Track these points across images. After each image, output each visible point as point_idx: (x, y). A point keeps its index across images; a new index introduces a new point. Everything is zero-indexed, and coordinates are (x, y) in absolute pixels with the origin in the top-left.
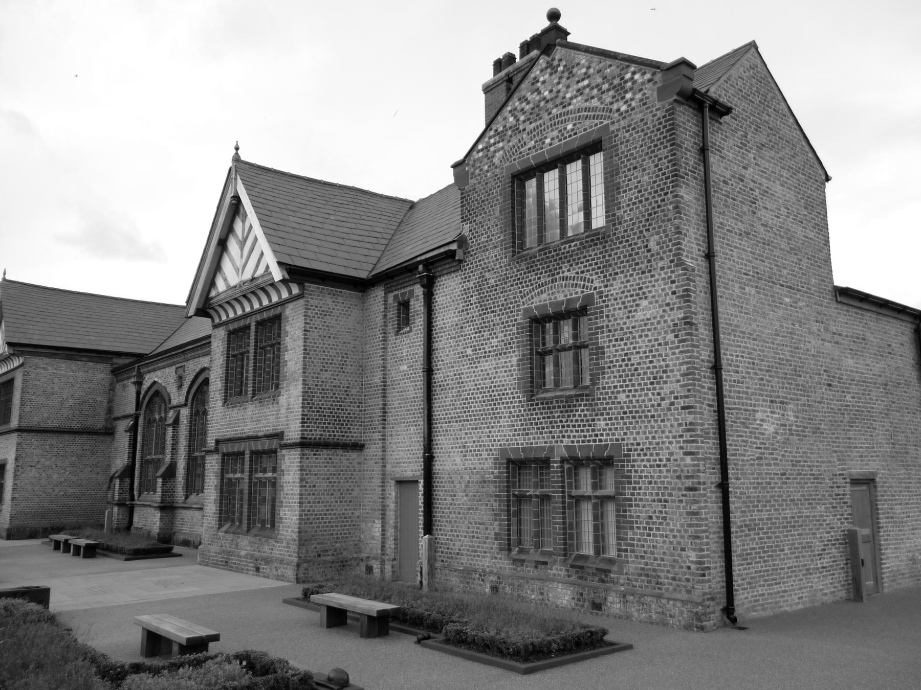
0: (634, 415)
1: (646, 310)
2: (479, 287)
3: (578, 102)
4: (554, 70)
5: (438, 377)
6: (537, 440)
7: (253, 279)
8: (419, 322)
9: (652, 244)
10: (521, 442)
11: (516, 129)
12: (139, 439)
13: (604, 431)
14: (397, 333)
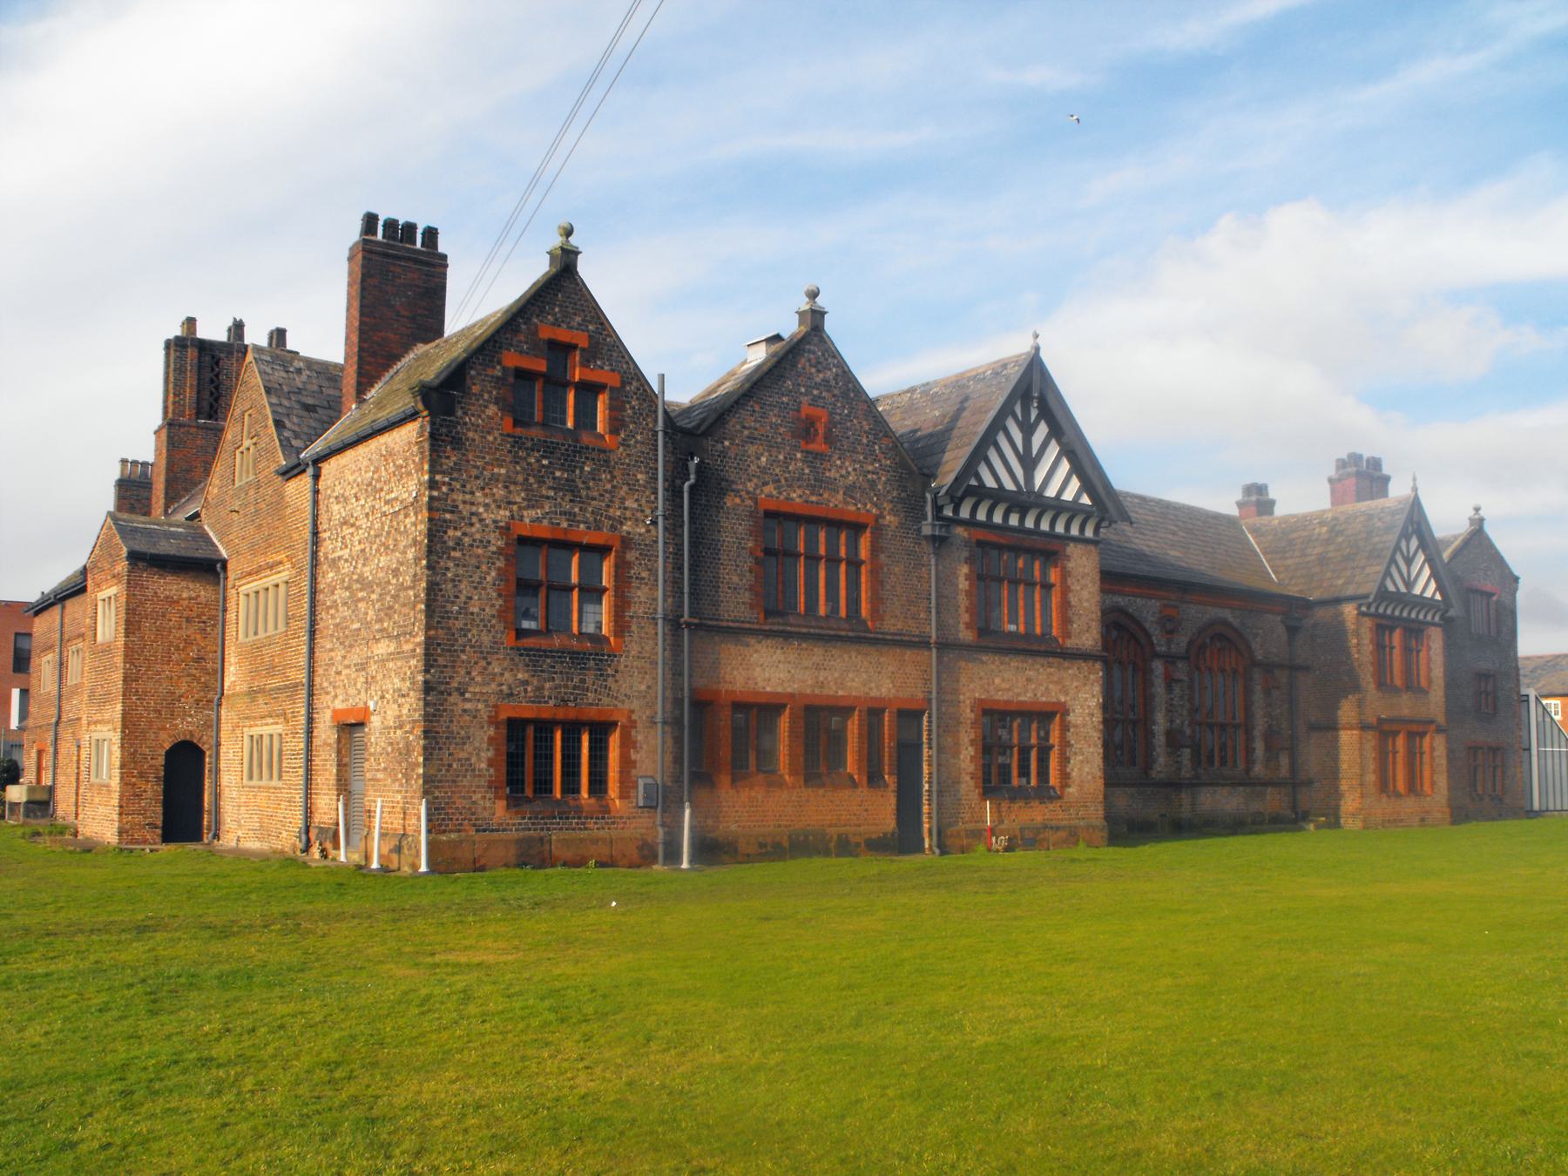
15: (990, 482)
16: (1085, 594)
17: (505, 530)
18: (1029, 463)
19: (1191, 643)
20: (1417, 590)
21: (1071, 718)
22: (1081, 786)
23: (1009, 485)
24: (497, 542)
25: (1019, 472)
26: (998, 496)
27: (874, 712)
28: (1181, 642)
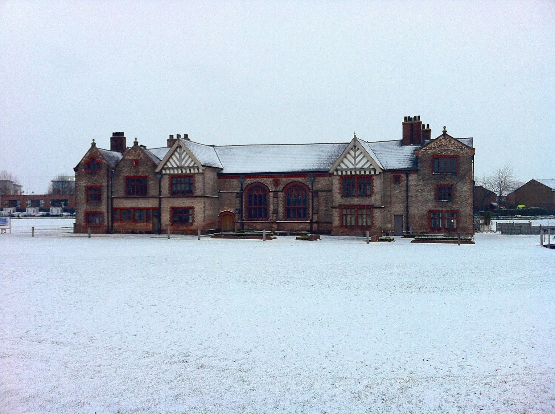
0: (461, 205)
1: (465, 189)
2: (424, 177)
3: (451, 148)
4: (446, 140)
5: (410, 194)
6: (438, 208)
7: (362, 168)
8: (404, 183)
9: (467, 178)
10: (434, 208)
11: (435, 148)
12: (244, 200)
13: (455, 208)
14: (395, 184)
15: (170, 166)
16: (200, 184)
17: (85, 187)
18: (180, 160)
19: (284, 188)
20: (359, 166)
21: (195, 209)
22: (198, 223)
23: (175, 166)
24: (84, 188)
25: (178, 163)
26: (173, 168)
27: (148, 209)
28: (281, 187)
